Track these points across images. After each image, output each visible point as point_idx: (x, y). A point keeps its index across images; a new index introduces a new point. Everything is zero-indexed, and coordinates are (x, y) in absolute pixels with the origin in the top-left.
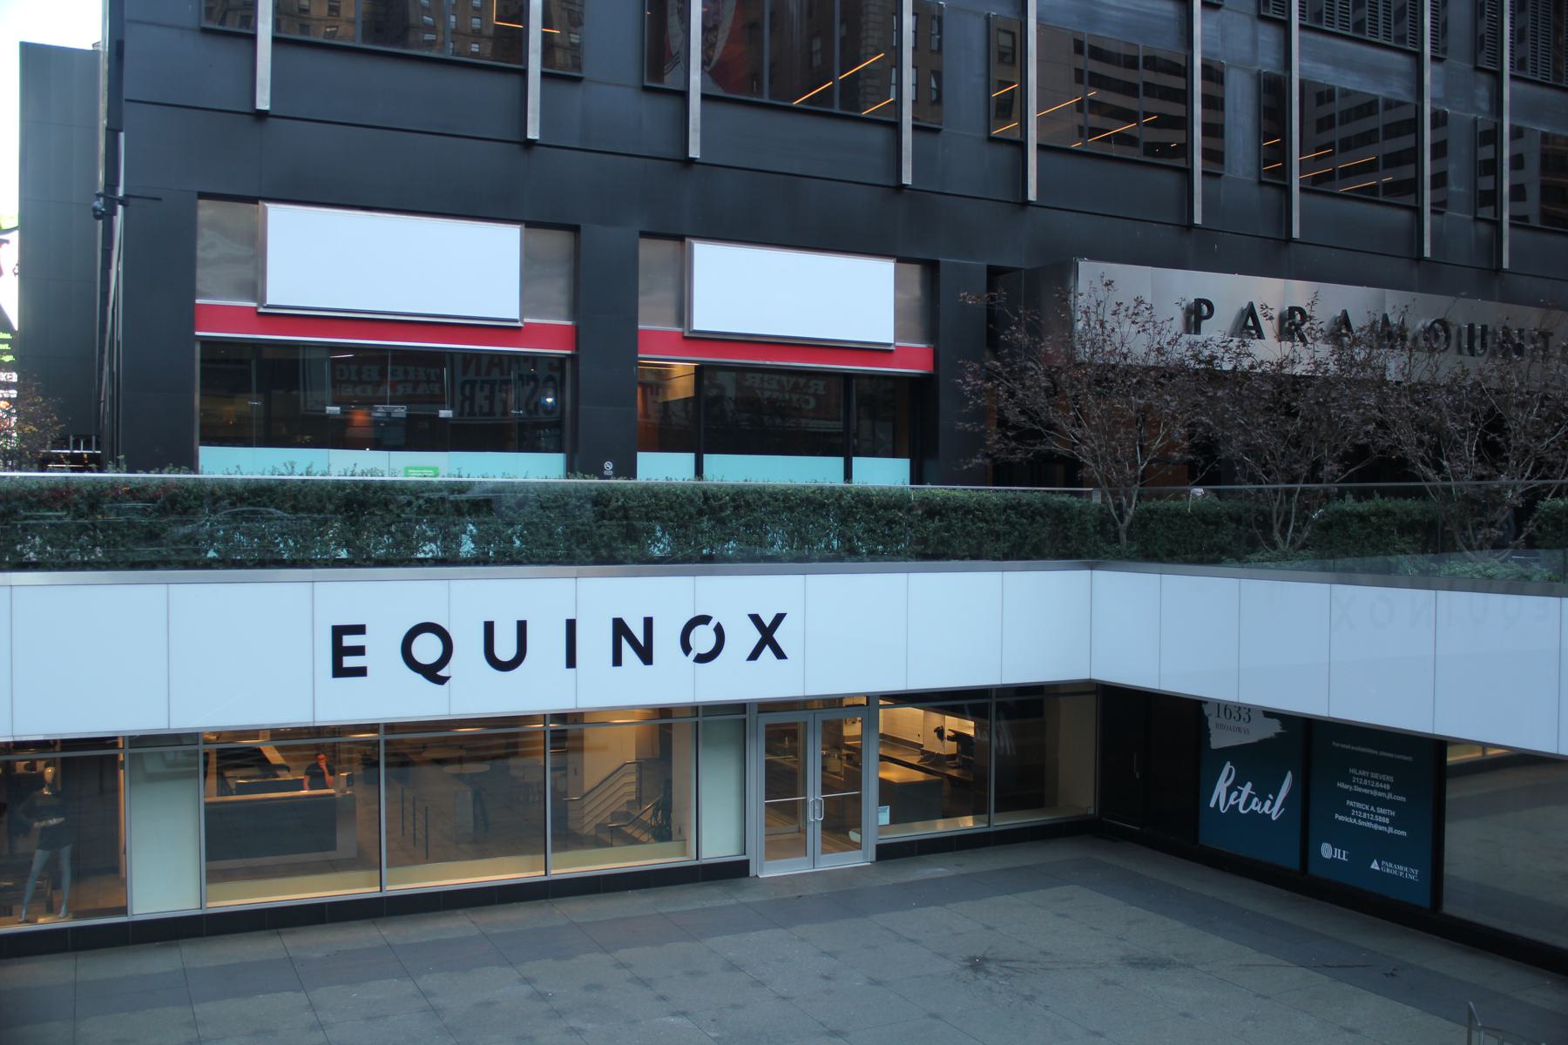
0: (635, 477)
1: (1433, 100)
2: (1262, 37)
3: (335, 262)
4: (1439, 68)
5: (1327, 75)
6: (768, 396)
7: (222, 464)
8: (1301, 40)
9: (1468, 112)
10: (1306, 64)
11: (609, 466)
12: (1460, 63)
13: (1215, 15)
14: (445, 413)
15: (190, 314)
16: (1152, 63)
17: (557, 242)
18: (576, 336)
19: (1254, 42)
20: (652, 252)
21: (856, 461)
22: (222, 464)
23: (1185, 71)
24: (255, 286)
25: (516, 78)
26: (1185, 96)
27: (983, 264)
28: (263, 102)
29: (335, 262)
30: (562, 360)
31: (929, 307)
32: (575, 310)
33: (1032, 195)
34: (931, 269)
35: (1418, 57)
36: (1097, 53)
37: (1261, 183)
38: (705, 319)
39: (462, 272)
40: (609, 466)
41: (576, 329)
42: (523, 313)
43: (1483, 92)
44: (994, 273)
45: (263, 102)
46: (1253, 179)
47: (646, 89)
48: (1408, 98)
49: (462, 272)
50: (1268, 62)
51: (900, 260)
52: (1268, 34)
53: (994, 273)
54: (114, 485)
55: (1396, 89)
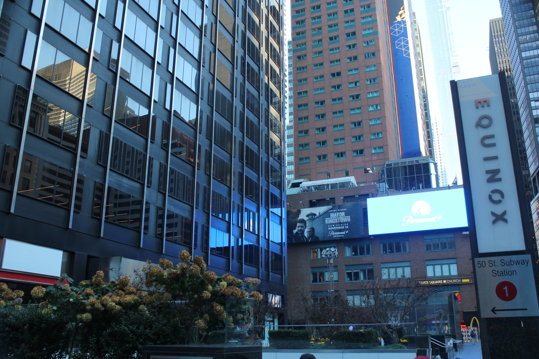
2: (159, 197)
13: (149, 189)
16: (61, 176)
23: (72, 179)
26: (71, 188)
27: (86, 254)
31: (69, 267)
33: (102, 235)
35: (192, 207)
36: (52, 172)
44: (89, 257)
48: (190, 218)
50: (160, 204)
51: (64, 251)
53: (89, 257)
55: (186, 215)
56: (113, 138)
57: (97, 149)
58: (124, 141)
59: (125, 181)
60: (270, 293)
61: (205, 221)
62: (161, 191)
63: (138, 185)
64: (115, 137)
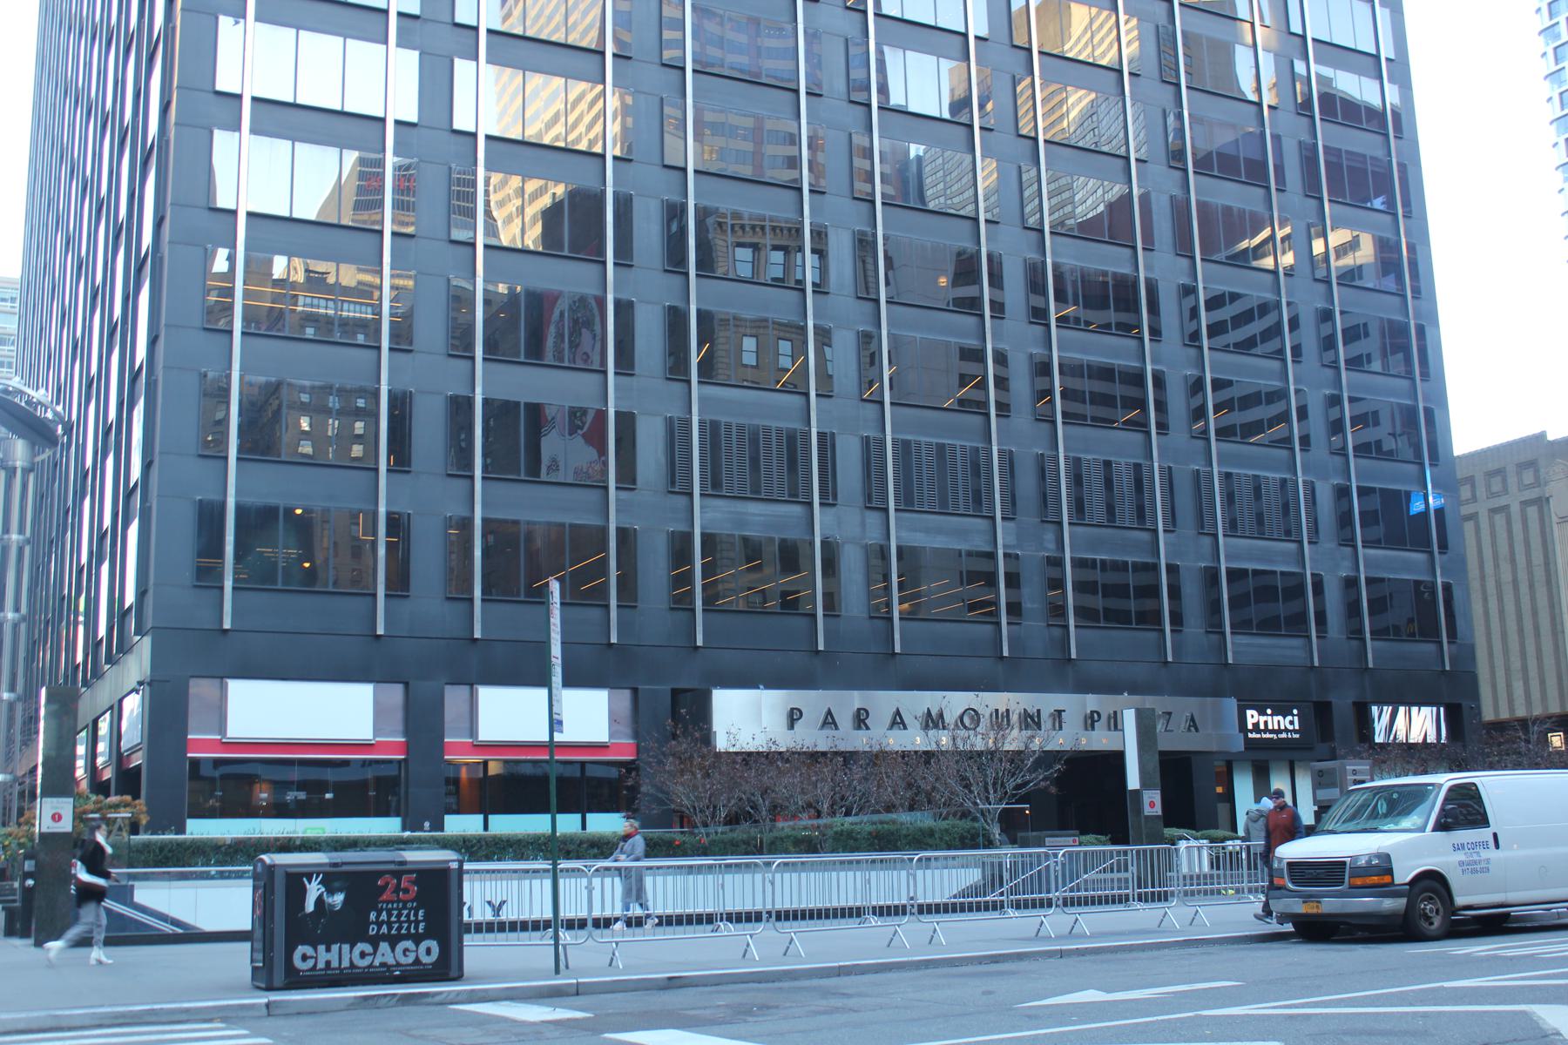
0: (442, 829)
1: (1005, 546)
3: (268, 712)
4: (1011, 524)
5: (918, 540)
6: (528, 781)
7: (200, 829)
8: (897, 519)
9: (1033, 555)
10: (904, 534)
11: (427, 824)
12: (1028, 518)
14: (328, 796)
15: (184, 744)
17: (396, 693)
18: (407, 747)
19: (863, 524)
20: (454, 697)
21: (589, 816)
22: (200, 829)
24: (222, 726)
25: (369, 599)
27: (667, 688)
28: (227, 625)
29: (268, 712)
30: (399, 761)
31: (639, 718)
32: (406, 732)
33: (700, 643)
34: (635, 691)
35: (993, 518)
37: (871, 618)
38: (486, 733)
39: (338, 713)
40: (427, 824)
41: (407, 743)
42: (376, 732)
43: (1049, 536)
45: (227, 625)
46: (865, 615)
47: (448, 599)
49: (338, 713)
50: (874, 537)
52: (873, 518)
54: (171, 841)
56: (701, 423)
57: (662, 459)
58: (734, 421)
59: (754, 508)
60: (1381, 703)
61: (1052, 546)
62: (873, 501)
63: (797, 510)
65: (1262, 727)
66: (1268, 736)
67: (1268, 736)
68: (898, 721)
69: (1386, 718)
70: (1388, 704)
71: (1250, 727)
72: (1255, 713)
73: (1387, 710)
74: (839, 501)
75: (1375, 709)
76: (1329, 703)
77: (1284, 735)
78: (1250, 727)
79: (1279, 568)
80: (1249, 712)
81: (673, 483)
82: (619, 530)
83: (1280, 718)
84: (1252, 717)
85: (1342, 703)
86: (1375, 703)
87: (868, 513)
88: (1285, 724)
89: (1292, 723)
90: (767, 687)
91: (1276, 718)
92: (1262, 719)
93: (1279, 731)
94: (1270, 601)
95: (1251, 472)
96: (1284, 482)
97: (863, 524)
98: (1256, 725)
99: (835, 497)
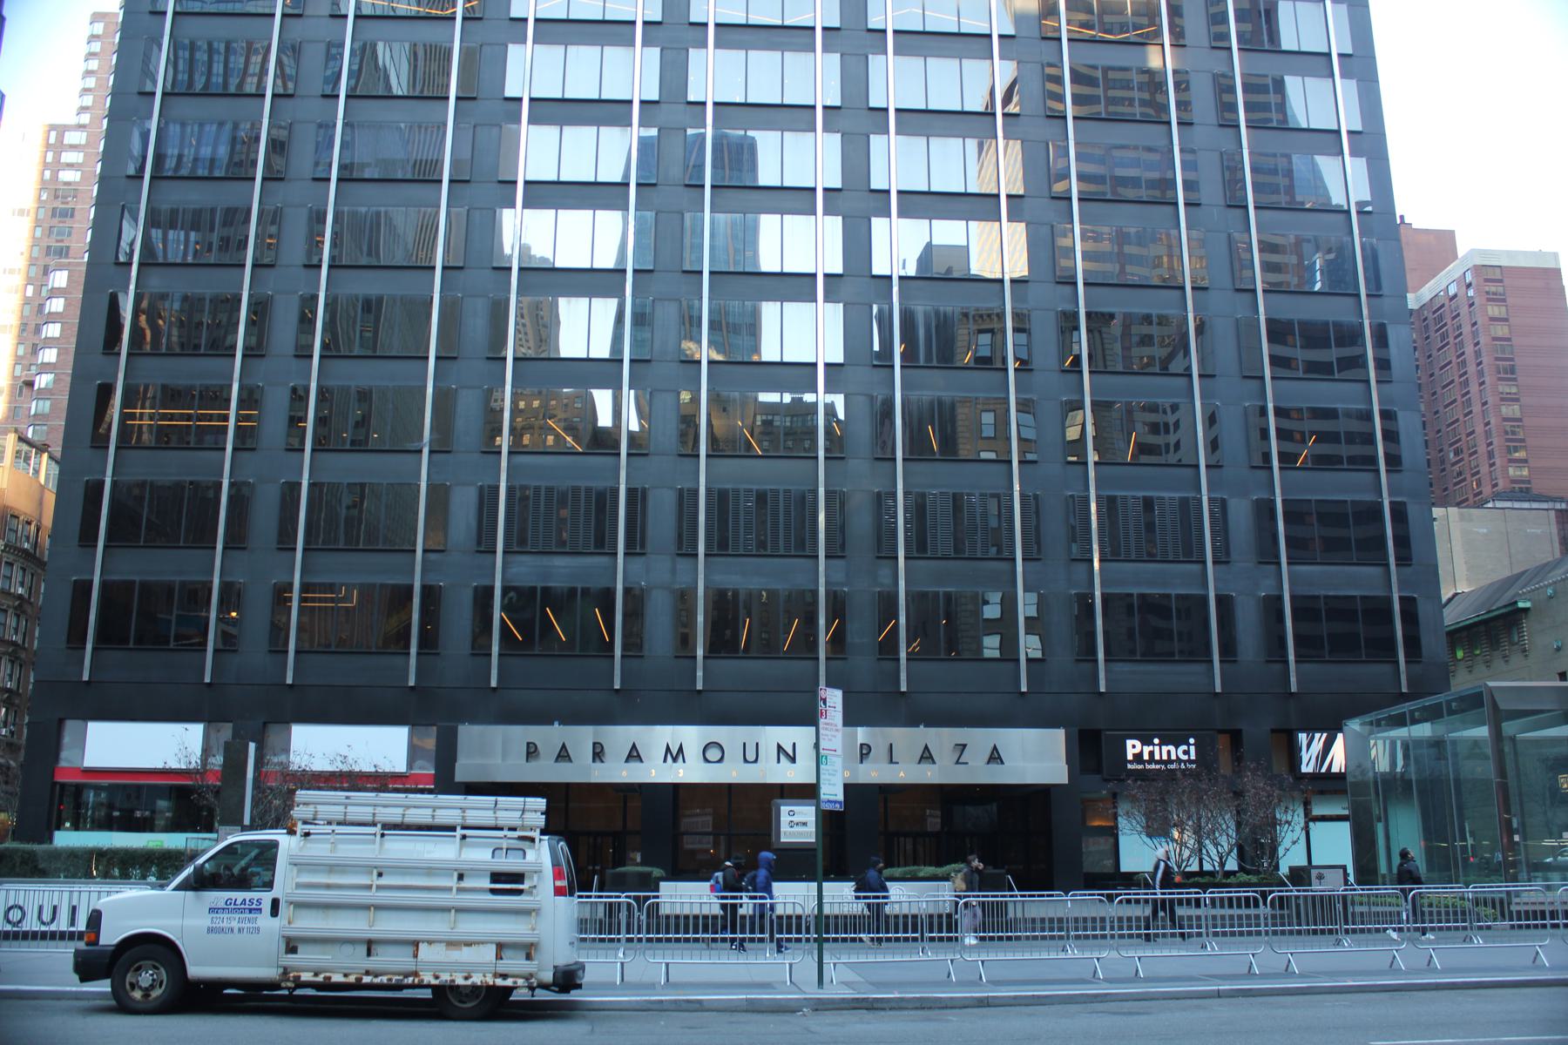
7: (66, 839)
13: (638, 562)
19: (674, 571)
22: (66, 839)
60: (1311, 729)
64: (517, 483)
65: (1146, 757)
66: (1153, 766)
67: (1153, 766)
68: (634, 755)
69: (1317, 745)
70: (1321, 730)
71: (1130, 757)
72: (1137, 743)
73: (1319, 739)
74: (649, 548)
75: (1303, 737)
76: (1240, 731)
77: (1173, 766)
78: (1130, 757)
79: (1173, 592)
80: (1129, 743)
81: (479, 543)
82: (424, 588)
83: (1171, 748)
84: (1133, 747)
85: (1257, 730)
86: (1303, 731)
87: (680, 560)
88: (1182, 753)
89: (1186, 752)
90: (563, 722)
91: (1165, 749)
92: (1147, 749)
93: (1169, 761)
94: (1158, 627)
95: (1141, 494)
96: (1184, 502)
97: (674, 571)
98: (1138, 757)
99: (643, 546)
